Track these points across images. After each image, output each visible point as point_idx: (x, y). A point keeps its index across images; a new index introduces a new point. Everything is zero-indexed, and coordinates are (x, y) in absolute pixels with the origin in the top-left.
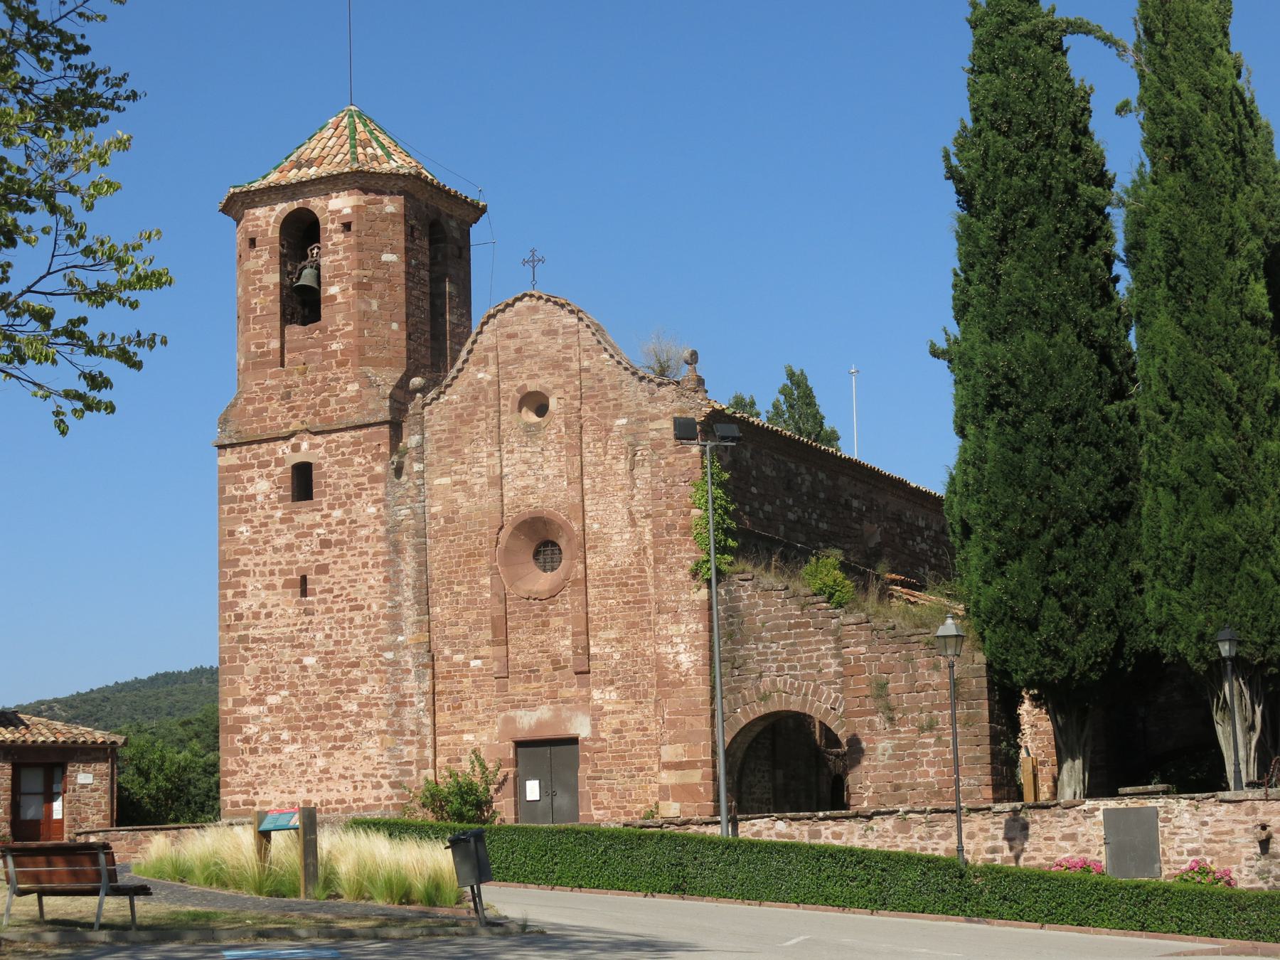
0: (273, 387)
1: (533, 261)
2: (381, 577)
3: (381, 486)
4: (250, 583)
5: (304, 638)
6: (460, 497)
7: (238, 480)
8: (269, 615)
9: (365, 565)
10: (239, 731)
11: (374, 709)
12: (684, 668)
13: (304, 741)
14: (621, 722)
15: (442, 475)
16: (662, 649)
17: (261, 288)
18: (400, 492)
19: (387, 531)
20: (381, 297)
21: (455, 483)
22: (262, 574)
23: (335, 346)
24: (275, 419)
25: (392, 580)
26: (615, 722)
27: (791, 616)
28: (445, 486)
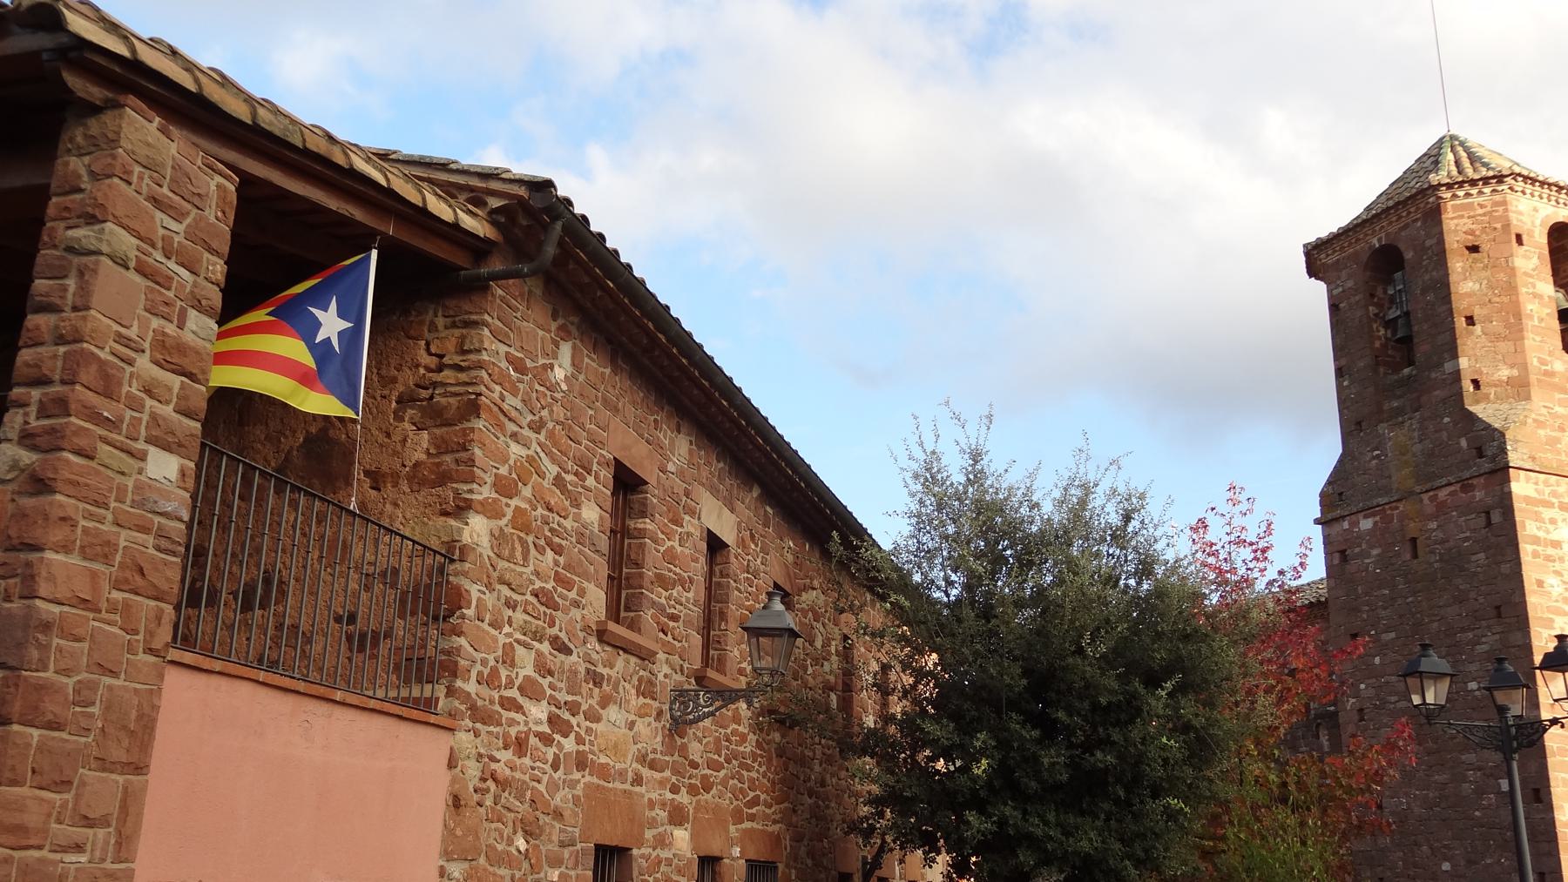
7: (1538, 518)
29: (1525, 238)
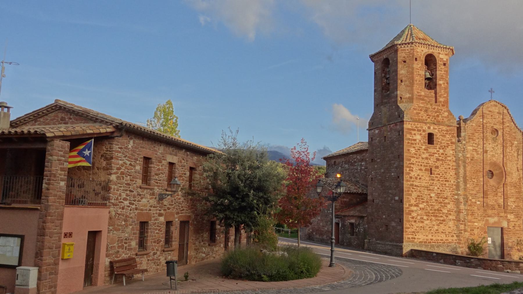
0: (422, 107)
2: (454, 173)
3: (454, 145)
4: (415, 168)
5: (431, 188)
7: (411, 134)
8: (420, 179)
11: (452, 213)
13: (431, 220)
17: (419, 74)
19: (456, 159)
21: (473, 149)
22: (418, 165)
24: (422, 117)
25: (457, 174)
26: (513, 224)
29: (418, 59)
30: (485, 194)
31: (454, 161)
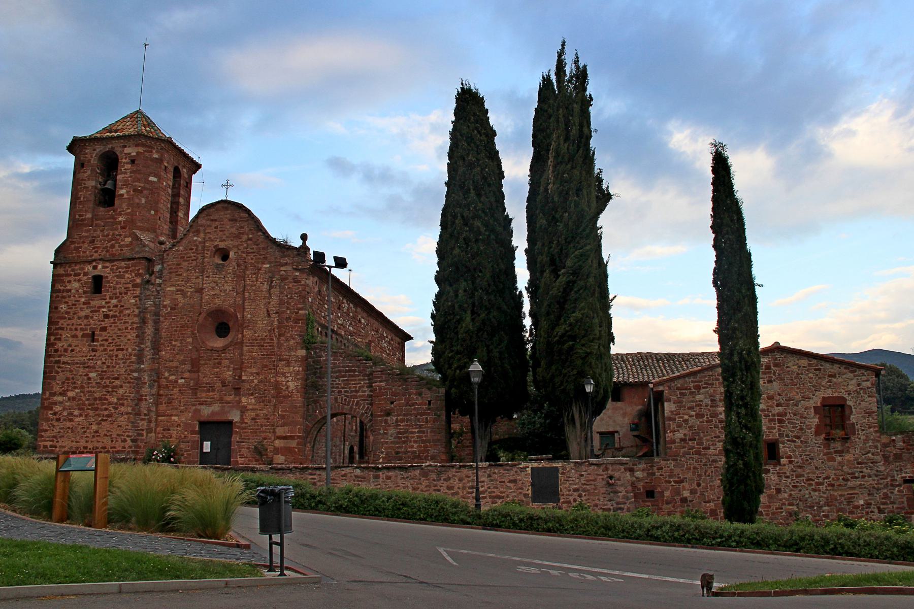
0: (86, 237)
1: (227, 186)
5: (91, 363)
6: (179, 297)
8: (72, 350)
9: (126, 328)
10: (51, 409)
12: (290, 389)
13: (86, 416)
14: (257, 415)
15: (171, 286)
16: (280, 379)
18: (148, 293)
20: (147, 197)
21: (178, 291)
22: (71, 329)
23: (120, 219)
25: (141, 337)
26: (253, 414)
27: (348, 366)
28: (173, 292)
30: (195, 366)
31: (135, 316)
